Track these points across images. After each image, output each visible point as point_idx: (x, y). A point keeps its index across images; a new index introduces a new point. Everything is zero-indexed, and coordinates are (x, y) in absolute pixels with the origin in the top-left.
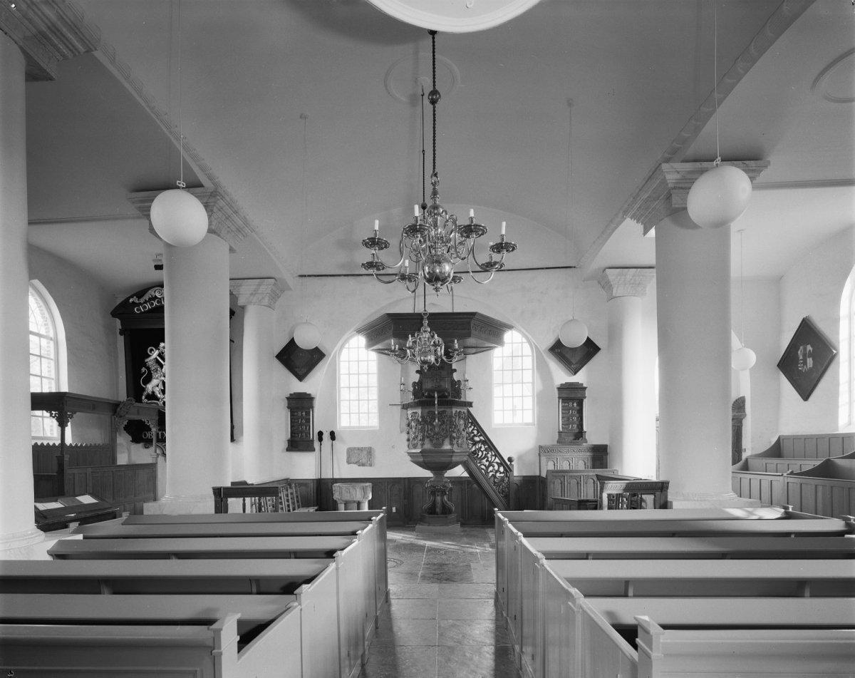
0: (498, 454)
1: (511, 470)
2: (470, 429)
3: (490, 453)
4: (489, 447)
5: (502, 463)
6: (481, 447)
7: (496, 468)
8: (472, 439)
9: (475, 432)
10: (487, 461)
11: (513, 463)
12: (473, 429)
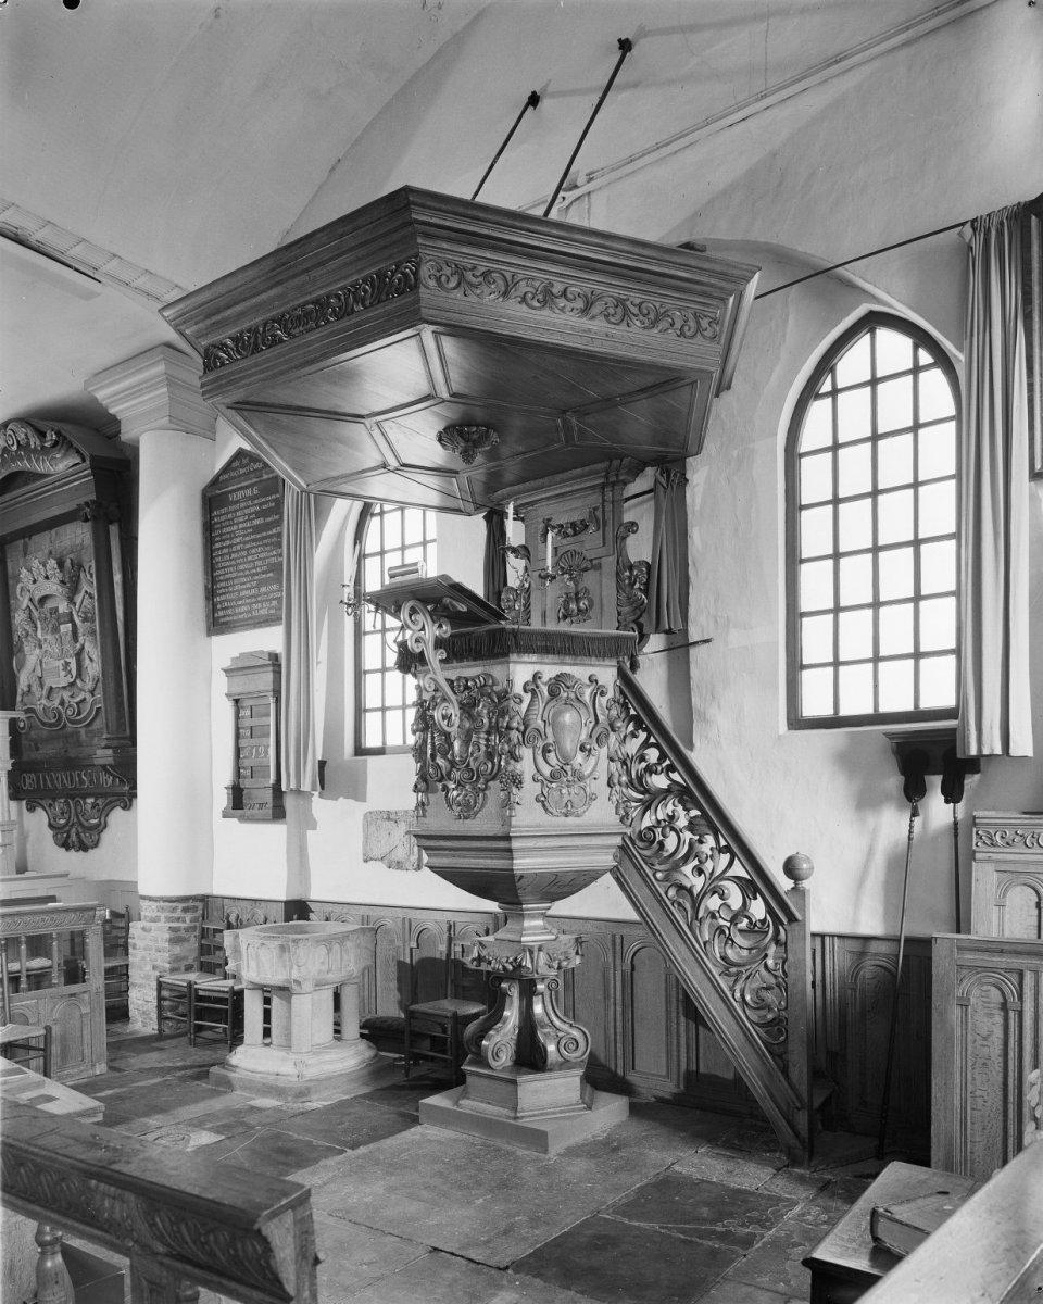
0: (739, 847)
1: (792, 919)
2: (632, 747)
3: (710, 840)
4: (704, 814)
5: (757, 883)
6: (672, 818)
7: (735, 898)
8: (638, 783)
9: (653, 755)
10: (699, 871)
11: (805, 884)
12: (646, 745)
